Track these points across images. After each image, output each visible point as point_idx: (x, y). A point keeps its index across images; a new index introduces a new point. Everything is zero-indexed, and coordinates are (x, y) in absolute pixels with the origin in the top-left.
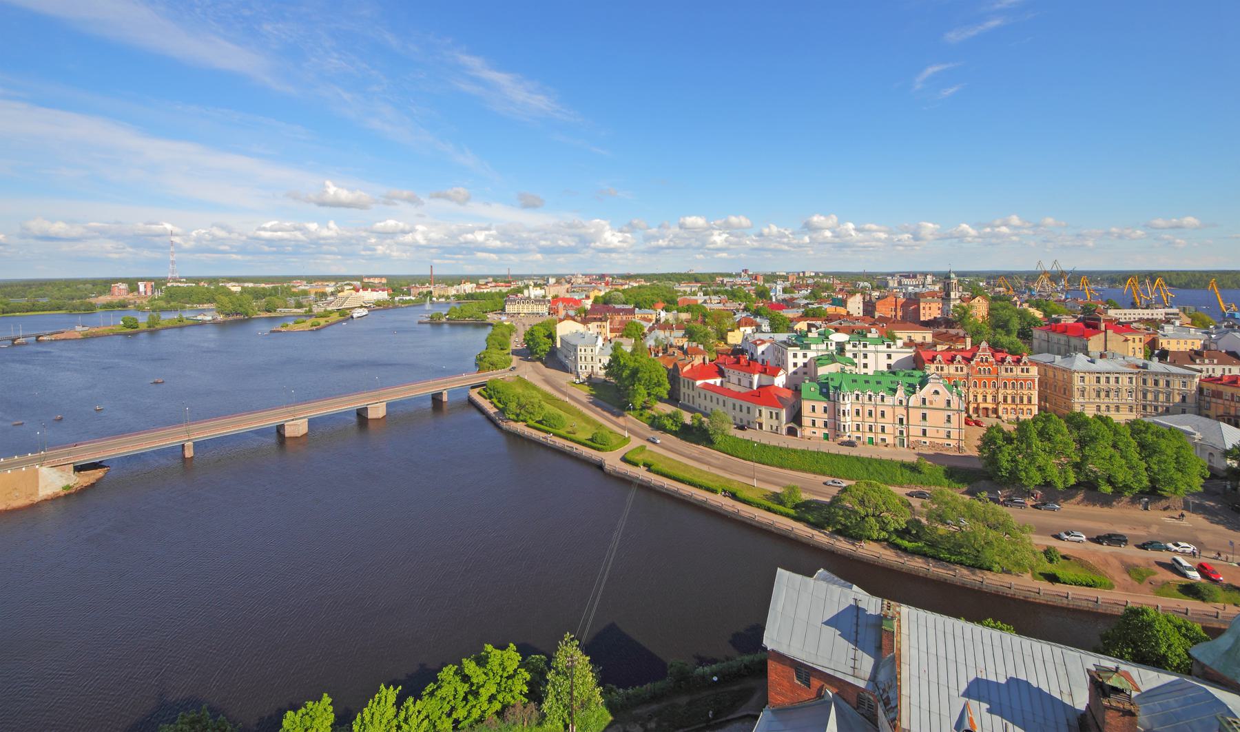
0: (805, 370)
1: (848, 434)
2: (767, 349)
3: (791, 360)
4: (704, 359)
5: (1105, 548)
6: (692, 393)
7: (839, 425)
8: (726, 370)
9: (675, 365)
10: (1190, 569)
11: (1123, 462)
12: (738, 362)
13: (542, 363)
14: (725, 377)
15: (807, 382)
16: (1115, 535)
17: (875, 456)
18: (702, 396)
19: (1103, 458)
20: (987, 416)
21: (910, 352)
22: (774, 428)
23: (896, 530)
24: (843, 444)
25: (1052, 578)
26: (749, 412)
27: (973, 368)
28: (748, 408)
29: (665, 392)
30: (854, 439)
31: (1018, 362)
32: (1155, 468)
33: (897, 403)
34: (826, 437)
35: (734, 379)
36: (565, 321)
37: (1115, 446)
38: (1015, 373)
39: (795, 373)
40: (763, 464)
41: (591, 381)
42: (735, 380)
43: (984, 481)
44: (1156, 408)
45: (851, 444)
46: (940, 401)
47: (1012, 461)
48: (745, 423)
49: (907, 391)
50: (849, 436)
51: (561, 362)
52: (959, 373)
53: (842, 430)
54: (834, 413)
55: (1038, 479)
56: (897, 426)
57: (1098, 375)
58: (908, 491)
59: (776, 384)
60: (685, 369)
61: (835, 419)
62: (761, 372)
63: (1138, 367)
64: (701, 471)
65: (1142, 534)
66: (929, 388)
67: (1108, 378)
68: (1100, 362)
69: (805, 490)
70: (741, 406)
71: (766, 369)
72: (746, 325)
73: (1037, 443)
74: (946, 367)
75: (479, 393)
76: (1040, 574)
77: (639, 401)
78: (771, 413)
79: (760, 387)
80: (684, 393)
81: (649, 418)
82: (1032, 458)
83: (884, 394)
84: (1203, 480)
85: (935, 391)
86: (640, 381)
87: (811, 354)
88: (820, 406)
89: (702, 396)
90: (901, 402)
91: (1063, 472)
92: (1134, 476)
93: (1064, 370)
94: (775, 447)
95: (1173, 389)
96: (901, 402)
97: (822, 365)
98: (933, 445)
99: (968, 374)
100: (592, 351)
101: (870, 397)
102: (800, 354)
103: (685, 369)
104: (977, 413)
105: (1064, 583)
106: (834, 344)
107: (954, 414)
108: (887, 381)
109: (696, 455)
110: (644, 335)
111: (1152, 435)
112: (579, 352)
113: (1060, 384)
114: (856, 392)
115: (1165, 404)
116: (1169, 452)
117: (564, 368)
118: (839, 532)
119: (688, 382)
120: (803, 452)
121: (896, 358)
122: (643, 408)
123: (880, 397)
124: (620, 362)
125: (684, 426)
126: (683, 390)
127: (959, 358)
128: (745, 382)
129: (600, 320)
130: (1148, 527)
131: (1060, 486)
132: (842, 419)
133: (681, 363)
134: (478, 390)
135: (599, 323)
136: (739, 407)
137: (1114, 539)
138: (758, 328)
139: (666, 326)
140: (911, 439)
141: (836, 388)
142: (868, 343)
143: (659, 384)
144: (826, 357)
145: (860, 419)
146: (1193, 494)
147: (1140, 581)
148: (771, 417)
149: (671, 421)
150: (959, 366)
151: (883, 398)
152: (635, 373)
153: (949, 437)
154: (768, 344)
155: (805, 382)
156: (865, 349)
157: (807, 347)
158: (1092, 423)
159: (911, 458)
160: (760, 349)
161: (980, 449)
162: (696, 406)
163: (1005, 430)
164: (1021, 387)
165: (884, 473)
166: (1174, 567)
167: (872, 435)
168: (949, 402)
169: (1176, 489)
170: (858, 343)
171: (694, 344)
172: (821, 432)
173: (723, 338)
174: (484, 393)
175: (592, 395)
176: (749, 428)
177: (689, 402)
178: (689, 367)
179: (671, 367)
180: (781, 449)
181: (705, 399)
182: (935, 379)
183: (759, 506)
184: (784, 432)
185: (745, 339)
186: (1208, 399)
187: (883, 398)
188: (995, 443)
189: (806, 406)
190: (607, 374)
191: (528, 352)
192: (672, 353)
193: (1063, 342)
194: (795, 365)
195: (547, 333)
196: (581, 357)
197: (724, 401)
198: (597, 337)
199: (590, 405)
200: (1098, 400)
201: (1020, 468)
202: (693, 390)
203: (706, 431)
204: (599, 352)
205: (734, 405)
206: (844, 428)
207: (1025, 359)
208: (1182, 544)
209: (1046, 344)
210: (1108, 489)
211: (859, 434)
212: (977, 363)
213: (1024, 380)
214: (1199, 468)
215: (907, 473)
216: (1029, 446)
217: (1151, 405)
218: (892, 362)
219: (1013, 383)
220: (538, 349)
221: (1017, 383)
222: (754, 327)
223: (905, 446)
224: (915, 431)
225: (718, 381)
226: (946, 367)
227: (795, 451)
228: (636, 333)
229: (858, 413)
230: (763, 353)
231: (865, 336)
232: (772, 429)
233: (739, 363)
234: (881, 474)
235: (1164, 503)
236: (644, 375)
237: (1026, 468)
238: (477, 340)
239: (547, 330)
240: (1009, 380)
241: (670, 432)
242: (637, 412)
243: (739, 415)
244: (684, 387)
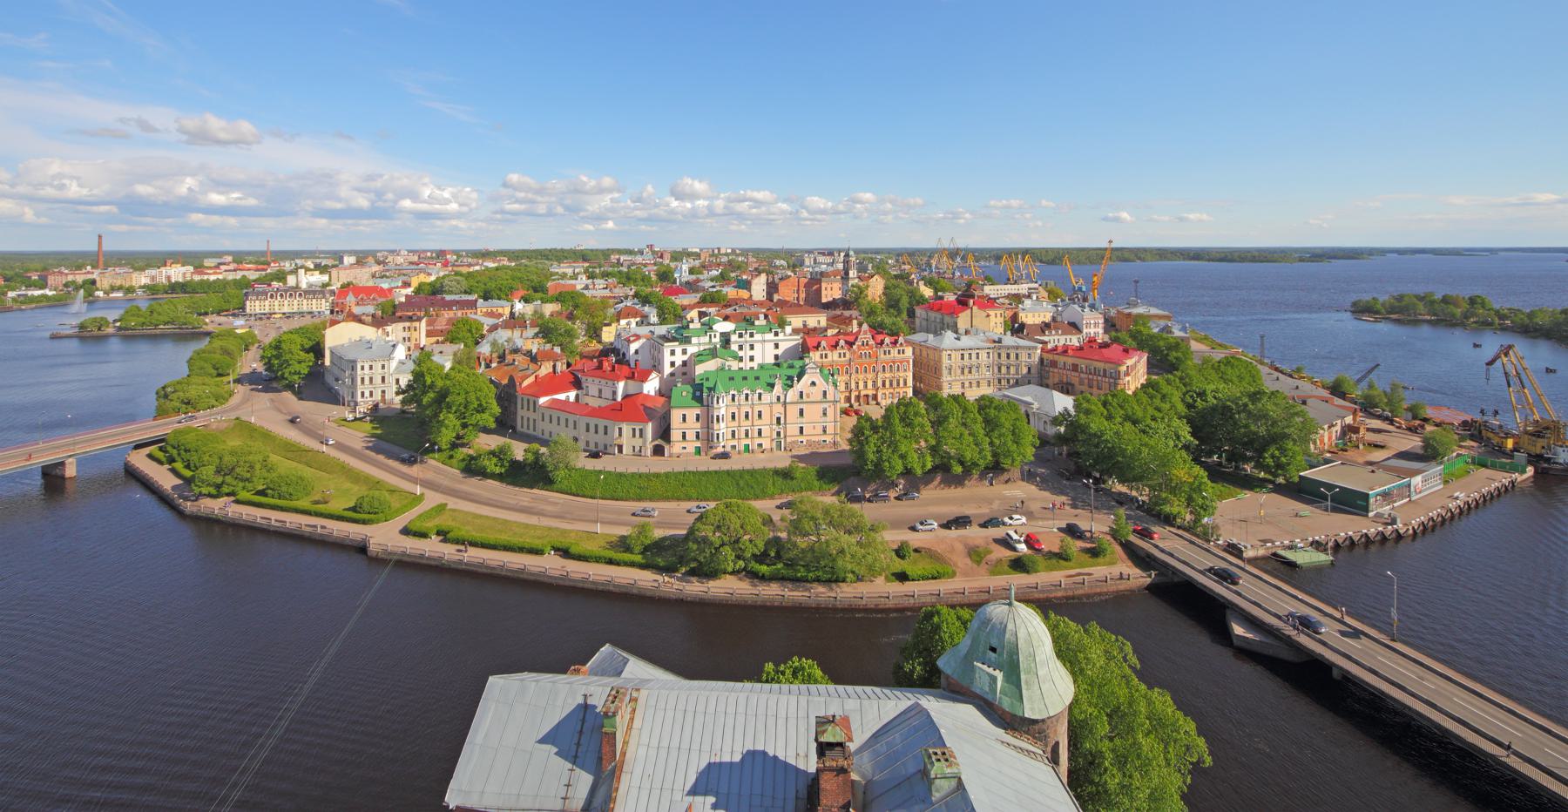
0: (684, 369)
1: (722, 444)
2: (642, 347)
3: (667, 359)
4: (554, 367)
5: (954, 533)
6: (532, 416)
7: (712, 434)
8: (583, 379)
9: (511, 379)
10: (1019, 542)
11: (971, 439)
12: (600, 367)
13: (294, 393)
14: (582, 389)
15: (679, 385)
16: (961, 518)
17: (748, 467)
18: (547, 418)
19: (954, 438)
20: (868, 404)
21: (797, 339)
22: (637, 449)
23: (754, 555)
24: (717, 457)
25: (902, 577)
26: (606, 433)
27: (855, 352)
28: (606, 427)
29: (492, 420)
30: (728, 449)
31: (895, 343)
32: (997, 442)
33: (775, 400)
34: (698, 451)
35: (593, 390)
36: (342, 324)
37: (964, 424)
38: (892, 355)
39: (672, 374)
40: (617, 500)
41: (375, 413)
42: (596, 393)
43: (852, 478)
44: (1008, 382)
45: (725, 456)
46: (816, 394)
47: (878, 452)
48: (601, 447)
49: (785, 385)
50: (724, 447)
51: (330, 389)
52: (842, 359)
53: (715, 440)
54: (708, 420)
55: (899, 468)
56: (774, 427)
57: (962, 352)
58: (778, 502)
59: (645, 392)
60: (526, 383)
61: (708, 428)
62: (627, 378)
63: (994, 342)
64: (527, 526)
65: (985, 511)
66: (806, 379)
67: (970, 354)
69: (660, 525)
70: (596, 426)
71: (633, 373)
72: (627, 316)
73: (899, 428)
74: (829, 354)
75: (150, 456)
76: (893, 574)
77: (446, 437)
78: (634, 430)
79: (626, 397)
80: (522, 417)
81: (463, 460)
82: (894, 446)
83: (762, 391)
84: (1034, 450)
85: (812, 382)
86: (450, 408)
87: (692, 350)
88: (692, 413)
89: (547, 418)
90: (778, 398)
91: (922, 456)
92: (980, 453)
93: (935, 349)
94: (633, 475)
96: (778, 398)
97: (701, 362)
98: (810, 443)
99: (850, 359)
100: (383, 367)
101: (747, 395)
102: (679, 350)
103: (526, 383)
104: (859, 401)
105: (913, 580)
106: (718, 335)
107: (830, 406)
108: (765, 378)
109: (525, 504)
110: (483, 337)
111: (995, 409)
112: (359, 371)
113: (932, 363)
114: (732, 392)
115: (1007, 376)
116: (1007, 425)
117: (334, 398)
118: (692, 573)
119: (528, 401)
120: (667, 475)
121: (784, 346)
122: (454, 446)
123: (730, 396)
124: (425, 382)
125: (515, 465)
126: (521, 413)
127: (842, 342)
128: (607, 393)
129: (410, 319)
130: (991, 504)
131: (919, 472)
132: (716, 426)
133: (520, 374)
134: (147, 450)
135: (407, 324)
136: (594, 426)
137: (961, 522)
138: (645, 319)
139: (514, 321)
140: (789, 440)
141: (710, 389)
142: (755, 332)
143: (481, 409)
144: (708, 352)
145: (735, 423)
146: (1026, 464)
147: (978, 563)
148: (634, 436)
149: (495, 460)
150: (842, 352)
151: (760, 395)
152: (442, 396)
153: (825, 431)
154: (642, 341)
155: (676, 386)
156: (752, 339)
157: (687, 341)
158: (945, 402)
159: (782, 461)
160: (634, 347)
161: (850, 441)
162: (538, 433)
163: (874, 418)
164: (898, 370)
165: (755, 486)
166: (1006, 543)
167: (748, 442)
168: (825, 393)
169: (1013, 461)
170: (744, 332)
171: (548, 346)
172: (692, 446)
173: (595, 333)
174: (160, 455)
175: (373, 436)
176: (605, 454)
177: (528, 428)
178: (531, 379)
179: (505, 382)
180: (640, 477)
181: (551, 422)
182: (812, 368)
183: (598, 560)
184: (649, 452)
185: (618, 336)
186: (1047, 369)
187: (760, 395)
188: (863, 434)
189: (676, 416)
190: (403, 402)
191: (270, 380)
192: (511, 362)
193: (938, 320)
194: (673, 364)
195: (308, 344)
196: (363, 379)
197: (575, 422)
198: (394, 346)
199: (368, 451)
200: (962, 378)
201: (884, 458)
202: (534, 411)
203: (543, 466)
204: (397, 368)
205: (588, 425)
206: (718, 438)
207: (901, 340)
208: (1015, 516)
209: (924, 323)
210: (958, 469)
211: (734, 443)
212: (859, 347)
214: (1031, 437)
215: (779, 480)
216: (893, 434)
217: (1004, 378)
218: (779, 352)
219: (891, 366)
220: (287, 371)
221: (892, 366)
222: (638, 319)
223: (783, 449)
224: (792, 430)
225: (572, 395)
226: (829, 354)
227: (657, 475)
228: (469, 335)
229: (733, 417)
230: (637, 352)
231: (753, 324)
232: (634, 451)
233: (602, 368)
234: (752, 487)
235: (1005, 476)
236: (456, 399)
237: (889, 457)
238: (171, 362)
239: (310, 339)
240: (887, 364)
241: (493, 476)
242: (446, 454)
243: (592, 437)
244: (522, 408)
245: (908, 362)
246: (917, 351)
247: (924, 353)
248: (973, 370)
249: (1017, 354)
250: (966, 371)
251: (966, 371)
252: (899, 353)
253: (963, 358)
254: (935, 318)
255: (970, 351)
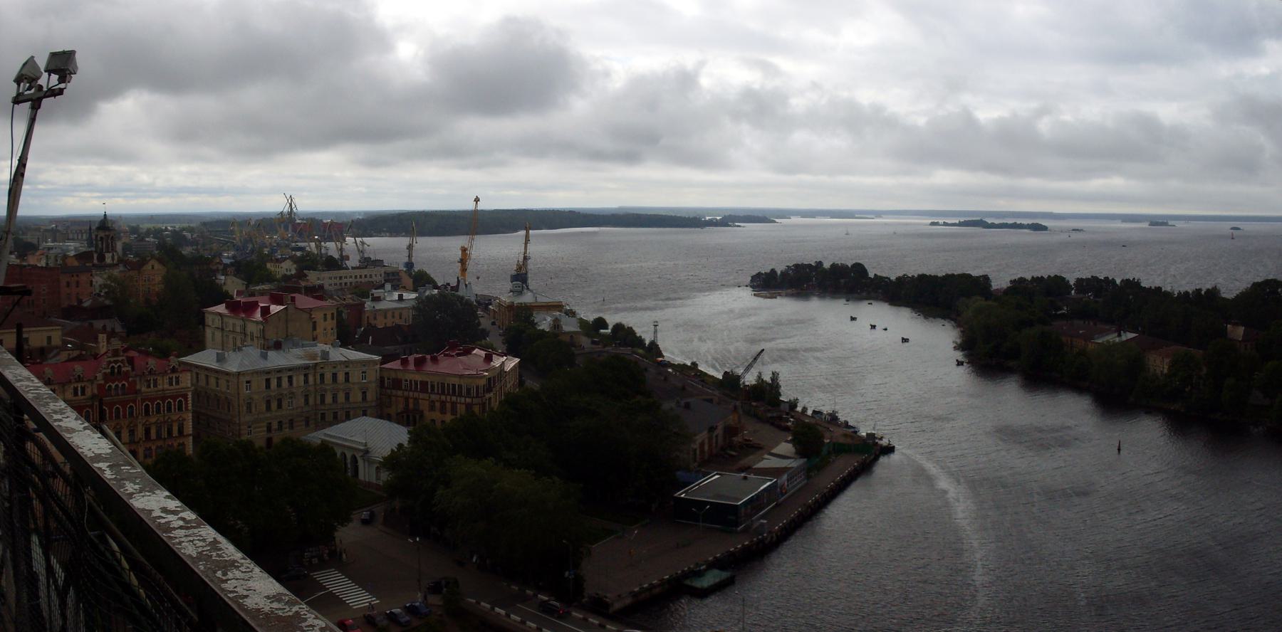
38: (160, 387)
52: (80, 397)
68: (271, 354)
95: (354, 384)
164: (169, 409)
186: (389, 391)
193: (238, 329)
209: (218, 334)
213: (171, 397)
240: (152, 400)
245: (185, 396)
246: (202, 377)
247: (212, 381)
248: (285, 404)
249: (347, 374)
250: (274, 405)
251: (274, 405)
252: (171, 384)
253: (268, 386)
254: (234, 325)
255: (279, 375)
